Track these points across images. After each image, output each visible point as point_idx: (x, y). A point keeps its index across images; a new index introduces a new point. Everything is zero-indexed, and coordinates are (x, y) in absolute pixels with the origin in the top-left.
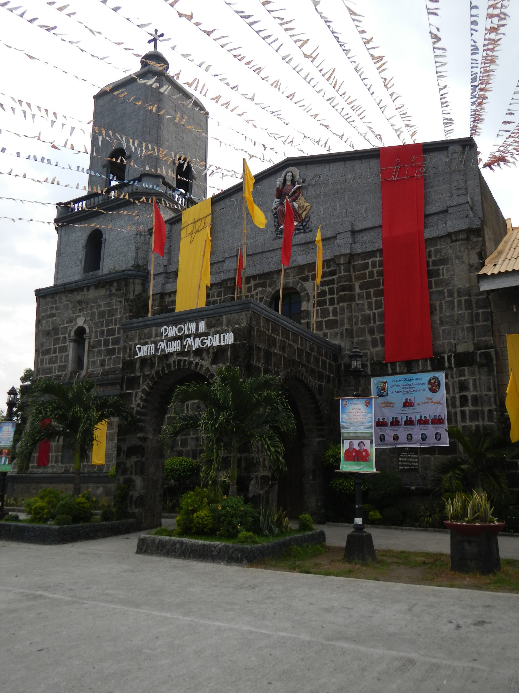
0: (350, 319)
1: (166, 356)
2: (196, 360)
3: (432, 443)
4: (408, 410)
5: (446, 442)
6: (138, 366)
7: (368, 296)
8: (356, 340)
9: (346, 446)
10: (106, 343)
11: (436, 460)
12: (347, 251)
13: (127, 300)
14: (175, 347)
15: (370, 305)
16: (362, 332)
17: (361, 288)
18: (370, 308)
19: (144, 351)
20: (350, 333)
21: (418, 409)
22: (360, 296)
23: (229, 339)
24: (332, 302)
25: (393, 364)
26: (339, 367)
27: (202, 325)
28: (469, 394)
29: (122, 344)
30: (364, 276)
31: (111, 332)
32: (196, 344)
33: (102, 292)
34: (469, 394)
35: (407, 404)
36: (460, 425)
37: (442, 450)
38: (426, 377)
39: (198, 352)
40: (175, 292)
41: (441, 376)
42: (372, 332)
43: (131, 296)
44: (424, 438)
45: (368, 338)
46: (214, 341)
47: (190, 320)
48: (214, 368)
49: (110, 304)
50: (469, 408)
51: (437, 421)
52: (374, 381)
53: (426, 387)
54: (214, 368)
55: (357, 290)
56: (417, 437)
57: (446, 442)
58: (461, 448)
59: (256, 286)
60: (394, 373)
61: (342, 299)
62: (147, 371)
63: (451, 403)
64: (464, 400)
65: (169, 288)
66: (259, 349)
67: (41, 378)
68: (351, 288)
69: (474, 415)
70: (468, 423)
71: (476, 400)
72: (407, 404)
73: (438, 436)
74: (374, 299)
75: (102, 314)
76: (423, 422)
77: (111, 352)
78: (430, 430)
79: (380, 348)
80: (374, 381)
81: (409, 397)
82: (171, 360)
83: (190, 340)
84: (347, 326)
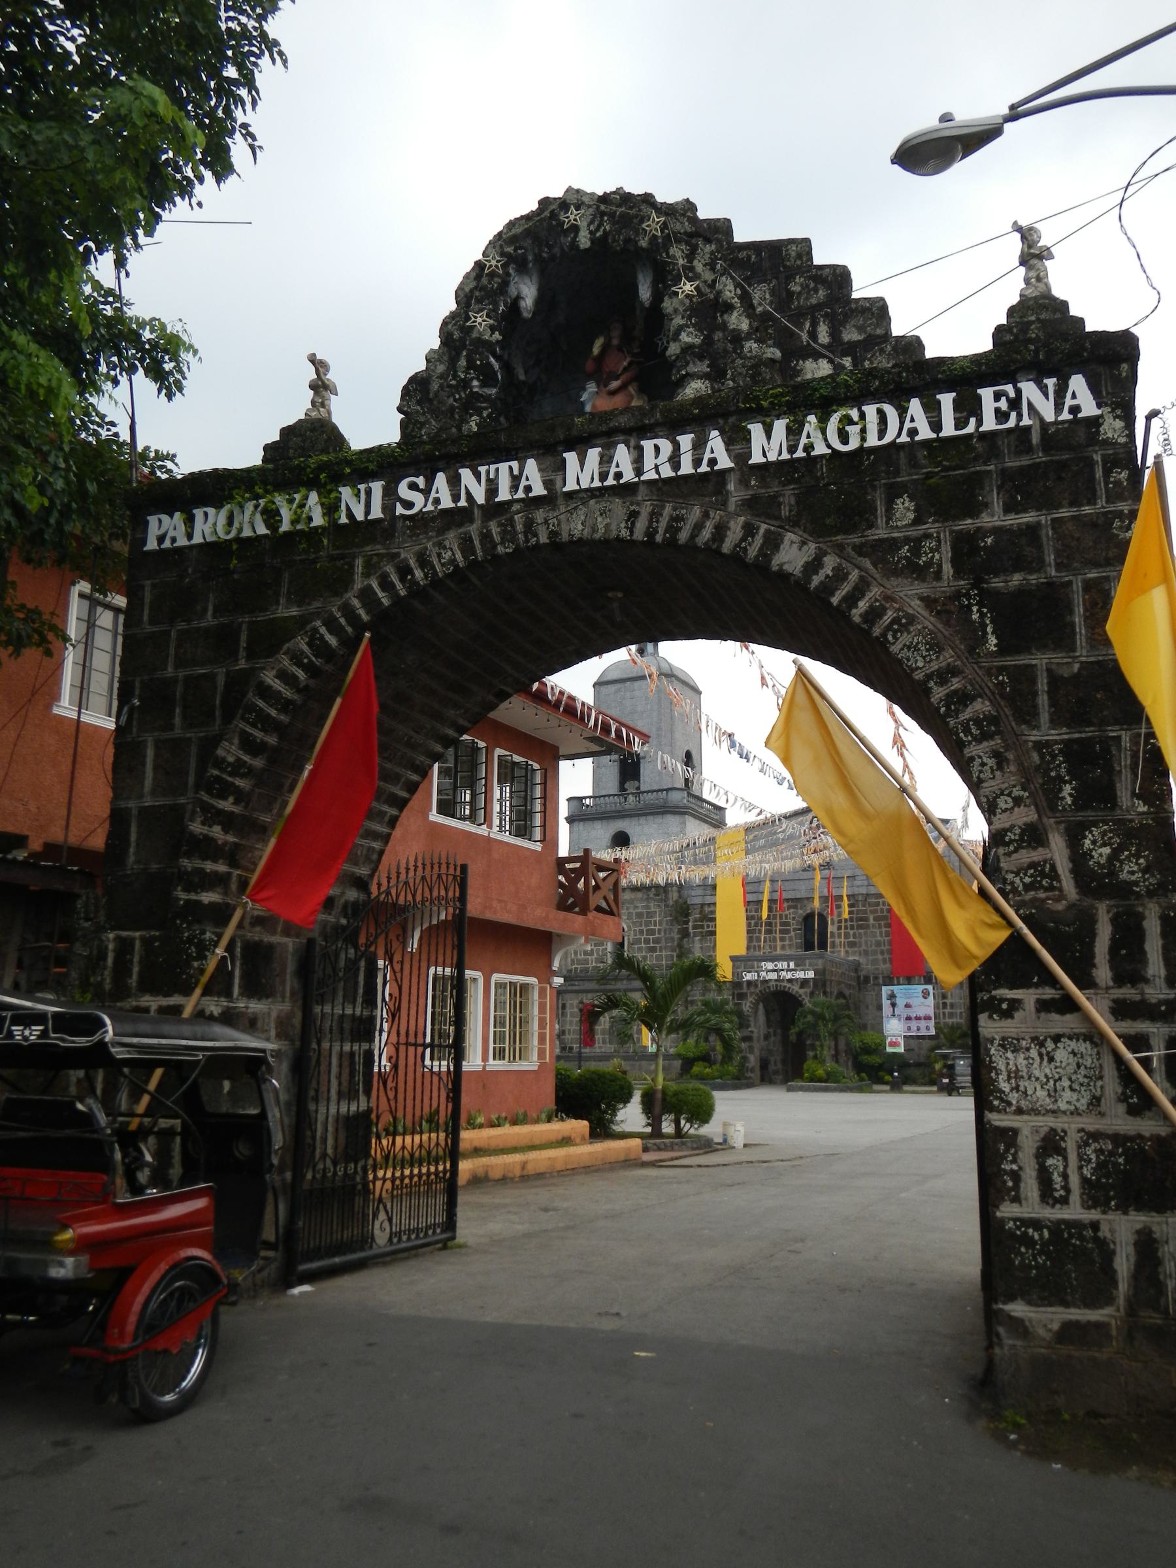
0: (866, 942)
1: (766, 981)
2: (788, 985)
3: (923, 1033)
4: (908, 1010)
5: (933, 1032)
6: (745, 985)
7: (880, 927)
8: (871, 958)
9: (889, 1040)
10: (647, 941)
11: (927, 1044)
12: (864, 891)
13: (667, 906)
14: (773, 976)
15: (881, 933)
16: (874, 953)
17: (875, 919)
18: (881, 935)
19: (749, 977)
20: (866, 953)
21: (914, 1009)
22: (874, 926)
23: (811, 974)
24: (852, 927)
25: (898, 978)
26: (859, 977)
27: (792, 965)
28: (948, 1001)
29: (663, 944)
30: (876, 911)
31: (651, 932)
32: (789, 976)
33: (640, 895)
34: (948, 1001)
35: (907, 1006)
36: (942, 1021)
37: (930, 1037)
38: (921, 987)
39: (790, 981)
40: (714, 904)
41: (930, 987)
42: (882, 953)
43: (671, 903)
44: (918, 1029)
45: (880, 957)
46: (801, 975)
47: (784, 960)
48: (801, 991)
49: (648, 907)
50: (948, 1011)
51: (927, 1018)
52: (884, 988)
53: (921, 994)
54: (801, 991)
55: (872, 921)
56: (914, 1028)
57: (933, 1032)
58: (942, 1036)
59: (789, 907)
60: (899, 984)
61: (860, 927)
62: (752, 989)
63: (936, 1007)
64: (945, 1005)
65: (708, 899)
66: (831, 981)
67: (576, 969)
68: (866, 919)
69: (951, 1015)
70: (947, 1020)
71: (952, 1006)
72: (907, 1006)
73: (928, 1028)
74: (884, 930)
75: (640, 915)
76: (918, 1018)
77: (653, 950)
78: (923, 1024)
79: (888, 965)
80: (884, 988)
81: (909, 1001)
82: (771, 984)
83: (784, 973)
84: (864, 947)
